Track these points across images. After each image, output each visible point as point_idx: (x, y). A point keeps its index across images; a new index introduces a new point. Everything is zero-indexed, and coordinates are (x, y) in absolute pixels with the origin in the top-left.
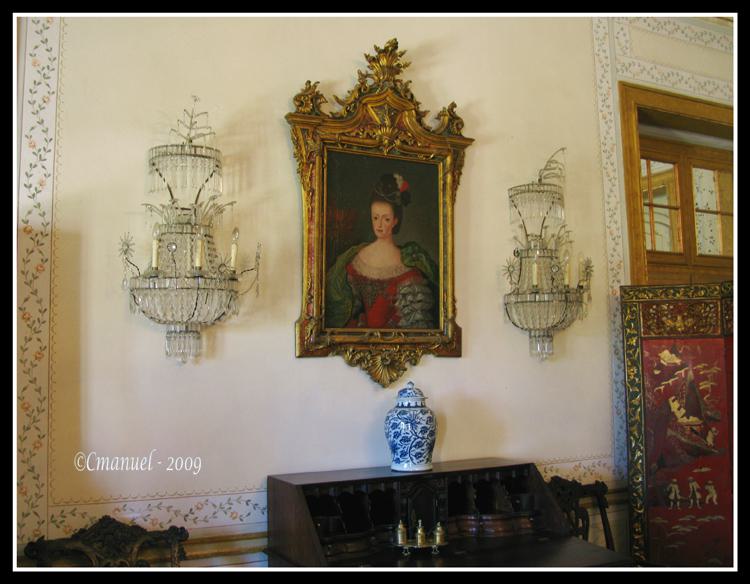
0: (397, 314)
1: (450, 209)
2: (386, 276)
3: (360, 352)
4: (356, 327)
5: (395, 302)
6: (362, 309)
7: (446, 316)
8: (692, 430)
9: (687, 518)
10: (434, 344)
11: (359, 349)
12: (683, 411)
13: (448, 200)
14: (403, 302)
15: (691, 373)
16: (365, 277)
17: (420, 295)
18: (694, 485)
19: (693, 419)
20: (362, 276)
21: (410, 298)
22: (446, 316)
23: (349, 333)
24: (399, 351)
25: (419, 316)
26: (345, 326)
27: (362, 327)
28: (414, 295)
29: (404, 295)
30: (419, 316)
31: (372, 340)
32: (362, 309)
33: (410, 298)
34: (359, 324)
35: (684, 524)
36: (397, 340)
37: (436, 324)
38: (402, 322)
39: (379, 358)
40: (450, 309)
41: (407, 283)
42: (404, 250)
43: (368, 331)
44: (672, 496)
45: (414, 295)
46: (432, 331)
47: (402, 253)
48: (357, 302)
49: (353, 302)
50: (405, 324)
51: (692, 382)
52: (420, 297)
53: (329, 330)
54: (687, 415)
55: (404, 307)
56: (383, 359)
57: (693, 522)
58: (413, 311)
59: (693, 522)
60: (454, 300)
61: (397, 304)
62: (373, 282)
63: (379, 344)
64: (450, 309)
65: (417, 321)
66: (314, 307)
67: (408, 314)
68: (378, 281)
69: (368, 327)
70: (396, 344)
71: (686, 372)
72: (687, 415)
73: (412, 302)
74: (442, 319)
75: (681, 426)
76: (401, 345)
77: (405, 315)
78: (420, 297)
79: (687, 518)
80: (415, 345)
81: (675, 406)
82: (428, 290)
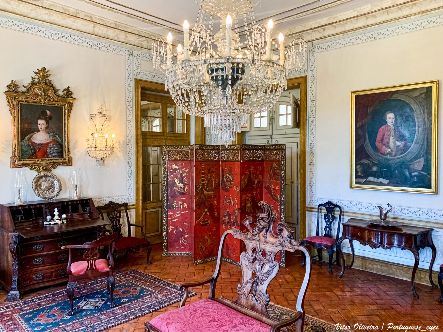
0: (48, 154)
1: (67, 121)
3: (34, 166)
4: (33, 158)
6: (35, 152)
7: (65, 154)
8: (181, 187)
9: (178, 212)
11: (34, 165)
12: (178, 182)
13: (66, 118)
14: (50, 150)
15: (181, 171)
18: (181, 203)
19: (181, 184)
21: (52, 149)
22: (65, 154)
23: (30, 160)
24: (49, 165)
25: (56, 154)
28: (54, 148)
29: (50, 148)
31: (38, 162)
32: (35, 152)
33: (52, 149)
35: (178, 214)
36: (47, 162)
38: (50, 156)
39: (41, 167)
40: (67, 152)
41: (52, 144)
43: (37, 159)
44: (174, 206)
45: (54, 148)
46: (61, 159)
48: (33, 151)
50: (51, 156)
51: (181, 174)
54: (179, 183)
56: (43, 168)
57: (180, 213)
58: (54, 152)
59: (180, 213)
60: (68, 149)
61: (48, 151)
62: (39, 144)
64: (67, 152)
65: (55, 156)
66: (16, 153)
69: (37, 158)
70: (47, 163)
71: (180, 171)
72: (179, 183)
73: (53, 150)
75: (178, 186)
77: (51, 154)
78: (56, 148)
79: (178, 212)
81: (176, 180)
82: (59, 146)
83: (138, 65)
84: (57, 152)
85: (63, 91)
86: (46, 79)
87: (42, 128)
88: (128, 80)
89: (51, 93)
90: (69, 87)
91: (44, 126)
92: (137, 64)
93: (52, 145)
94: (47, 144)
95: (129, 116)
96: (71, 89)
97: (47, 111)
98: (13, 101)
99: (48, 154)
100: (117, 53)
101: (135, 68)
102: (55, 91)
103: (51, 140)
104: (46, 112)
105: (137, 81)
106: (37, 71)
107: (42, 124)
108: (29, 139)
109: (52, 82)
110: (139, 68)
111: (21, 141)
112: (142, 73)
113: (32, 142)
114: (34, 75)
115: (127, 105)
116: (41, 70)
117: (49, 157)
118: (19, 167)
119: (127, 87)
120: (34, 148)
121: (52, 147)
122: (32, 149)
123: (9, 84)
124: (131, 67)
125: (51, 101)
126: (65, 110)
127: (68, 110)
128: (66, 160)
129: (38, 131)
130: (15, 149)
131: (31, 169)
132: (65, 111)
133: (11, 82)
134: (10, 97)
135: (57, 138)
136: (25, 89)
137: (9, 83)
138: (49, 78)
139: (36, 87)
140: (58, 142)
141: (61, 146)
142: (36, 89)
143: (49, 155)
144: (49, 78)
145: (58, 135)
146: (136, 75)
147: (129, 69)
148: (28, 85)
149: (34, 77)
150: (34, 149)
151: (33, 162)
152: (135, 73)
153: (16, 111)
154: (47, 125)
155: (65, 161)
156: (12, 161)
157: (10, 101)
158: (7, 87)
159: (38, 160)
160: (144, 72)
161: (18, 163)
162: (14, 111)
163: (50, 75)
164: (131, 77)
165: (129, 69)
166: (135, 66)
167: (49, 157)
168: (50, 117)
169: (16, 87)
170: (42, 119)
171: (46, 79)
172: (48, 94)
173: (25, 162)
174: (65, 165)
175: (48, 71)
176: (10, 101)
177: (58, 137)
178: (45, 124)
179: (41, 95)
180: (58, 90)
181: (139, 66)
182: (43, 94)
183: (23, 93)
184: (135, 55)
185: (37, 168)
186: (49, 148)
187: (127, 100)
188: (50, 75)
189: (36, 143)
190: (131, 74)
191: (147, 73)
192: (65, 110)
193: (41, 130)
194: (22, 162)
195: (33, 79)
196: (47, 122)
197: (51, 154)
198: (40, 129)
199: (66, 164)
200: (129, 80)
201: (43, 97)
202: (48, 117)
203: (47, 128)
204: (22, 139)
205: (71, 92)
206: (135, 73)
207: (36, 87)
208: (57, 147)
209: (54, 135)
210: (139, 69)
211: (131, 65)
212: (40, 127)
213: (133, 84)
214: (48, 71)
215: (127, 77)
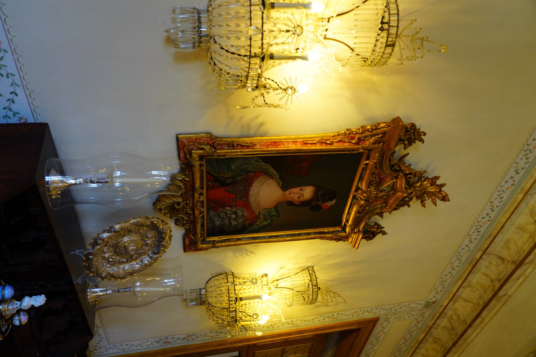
0: (220, 209)
2: (252, 199)
5: (231, 206)
7: (218, 242)
10: (194, 236)
16: (251, 186)
17: (235, 223)
20: (253, 182)
24: (187, 213)
25: (218, 223)
27: (207, 184)
28: (235, 219)
29: (235, 213)
30: (218, 223)
31: (196, 195)
33: (233, 216)
34: (210, 183)
37: (210, 234)
39: (180, 200)
41: (245, 214)
42: (273, 210)
43: (204, 191)
45: (235, 219)
46: (205, 235)
47: (271, 209)
48: (229, 181)
49: (229, 178)
50: (211, 215)
52: (234, 223)
53: (204, 163)
55: (226, 213)
56: (178, 204)
58: (223, 219)
61: (229, 208)
63: (193, 198)
65: (214, 222)
67: (220, 216)
69: (207, 190)
70: (193, 210)
73: (230, 218)
74: (216, 239)
76: (194, 214)
77: (218, 214)
78: (234, 223)
80: (193, 222)
87: (292, 195)
90: (384, 233)
92: (406, 316)
93: (243, 215)
94: (247, 205)
97: (334, 201)
100: (435, 287)
101: (398, 316)
103: (257, 213)
104: (332, 200)
106: (438, 182)
107: (303, 195)
109: (406, 207)
113: (256, 177)
117: (211, 211)
118: (182, 155)
121: (237, 216)
128: (202, 244)
129: (284, 188)
135: (261, 222)
136: (397, 156)
145: (269, 224)
151: (198, 184)
152: (389, 316)
154: (297, 203)
156: (200, 139)
158: (413, 125)
160: (388, 327)
161: (195, 156)
167: (211, 211)
168: (318, 208)
170: (315, 193)
174: (187, 242)
177: (265, 223)
178: (301, 199)
184: (424, 311)
186: (234, 210)
189: (250, 185)
190: (388, 311)
191: (386, 330)
193: (287, 192)
194: (197, 164)
197: (218, 214)
198: (290, 190)
202: (319, 203)
203: (290, 203)
209: (271, 216)
210: (396, 320)
212: (297, 190)
213: (368, 316)
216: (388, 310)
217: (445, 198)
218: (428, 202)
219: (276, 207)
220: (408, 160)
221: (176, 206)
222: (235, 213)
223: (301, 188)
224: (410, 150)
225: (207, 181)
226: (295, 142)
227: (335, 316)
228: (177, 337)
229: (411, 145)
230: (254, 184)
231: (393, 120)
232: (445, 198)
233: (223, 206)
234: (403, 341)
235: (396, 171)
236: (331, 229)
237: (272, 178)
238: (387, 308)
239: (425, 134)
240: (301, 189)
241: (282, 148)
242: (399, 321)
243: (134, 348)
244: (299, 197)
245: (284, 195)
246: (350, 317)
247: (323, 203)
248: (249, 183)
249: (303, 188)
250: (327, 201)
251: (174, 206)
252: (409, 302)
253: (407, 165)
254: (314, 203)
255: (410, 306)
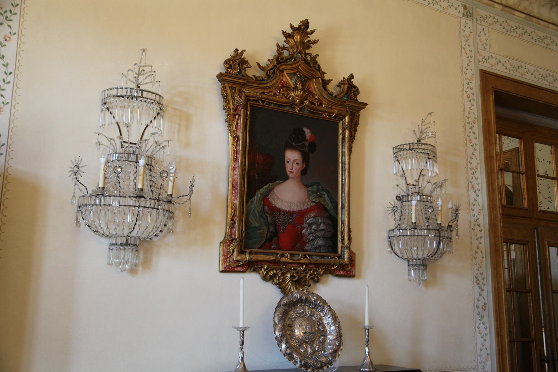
0: (304, 239)
1: (347, 158)
2: (295, 209)
3: (273, 269)
5: (302, 229)
6: (275, 234)
7: (343, 243)
10: (334, 266)
11: (272, 266)
13: (346, 151)
16: (279, 209)
17: (322, 225)
20: (275, 207)
21: (314, 227)
22: (343, 243)
23: (265, 254)
24: (305, 270)
25: (321, 242)
26: (261, 248)
27: (274, 249)
28: (318, 225)
29: (310, 225)
30: (321, 242)
31: (283, 259)
32: (275, 234)
33: (314, 227)
34: (273, 246)
36: (303, 261)
37: (335, 250)
38: (308, 246)
39: (289, 275)
40: (346, 238)
41: (313, 215)
42: (310, 189)
43: (280, 252)
45: (318, 225)
46: (332, 255)
47: (308, 191)
48: (272, 229)
49: (268, 229)
52: (322, 227)
53: (248, 251)
55: (309, 234)
56: (292, 277)
58: (317, 237)
60: (350, 231)
61: (304, 231)
62: (285, 213)
63: (289, 263)
64: (346, 238)
65: (320, 246)
66: (236, 231)
67: (313, 240)
68: (289, 212)
69: (279, 249)
70: (302, 264)
73: (316, 230)
74: (340, 245)
76: (306, 264)
77: (310, 241)
78: (322, 227)
80: (317, 265)
82: (328, 221)
83: (484, 41)
84: (324, 238)
85: (339, 85)
86: (307, 51)
87: (294, 170)
88: (467, 71)
89: (314, 86)
90: (352, 76)
91: (297, 167)
92: (483, 38)
93: (314, 217)
94: (302, 214)
95: (473, 157)
96: (355, 81)
97: (306, 130)
98: (237, 98)
99: (304, 239)
100: (442, 9)
101: (480, 47)
102: (325, 83)
103: (312, 204)
104: (304, 132)
105: (485, 76)
106: (290, 31)
107: (294, 161)
108: (265, 198)
109: (318, 59)
110: (487, 47)
111: (247, 202)
112: (494, 59)
113: (269, 204)
114: (282, 40)
115: (468, 130)
116: (299, 29)
117: (306, 248)
118: (239, 269)
119: (465, 89)
120: (274, 221)
121: (314, 223)
122: (268, 225)
123: (229, 57)
124: (471, 42)
125: (315, 104)
126: (344, 130)
127: (350, 132)
128: (344, 259)
129: (285, 178)
130: (232, 220)
131: (265, 278)
132: (343, 133)
133: (233, 54)
134: (231, 88)
135: (324, 200)
136: (259, 73)
137: (228, 54)
138: (313, 51)
139: (285, 69)
140: (326, 210)
141: (333, 221)
142: (285, 73)
143: (305, 243)
144: (313, 51)
145: (328, 193)
146: (481, 63)
147: (468, 48)
148: (269, 63)
149: (281, 45)
150: (275, 224)
151: (272, 258)
152: (480, 59)
153: (241, 122)
154: (305, 166)
155: (341, 261)
156: (224, 252)
157: (230, 97)
158: (226, 62)
159: (283, 255)
160: (498, 57)
161: (239, 258)
162: (237, 124)
163: (315, 42)
164: (472, 65)
165: (468, 48)
166: (479, 43)
167: (306, 248)
168: (312, 146)
169: (245, 66)
170: (293, 148)
171: (307, 51)
172: (308, 88)
173: (254, 257)
174: (342, 273)
175: (312, 32)
176: (230, 97)
177: (326, 196)
178: (300, 162)
179: (296, 88)
180: (329, 81)
181: (488, 43)
182: (299, 86)
183: (259, 80)
184: (478, 18)
185: (279, 277)
186: (307, 225)
187: (467, 120)
188: (315, 42)
189: (279, 210)
190: (472, 60)
191: (503, 60)
192: (344, 130)
193: (290, 175)
194: (247, 257)
195: (280, 49)
196: (305, 158)
197: (310, 241)
198: (288, 173)
199: (344, 270)
200: (470, 73)
201: (299, 93)
202: (307, 144)
203: (304, 172)
204: (250, 195)
205: (355, 87)
206: (480, 59)
207: (285, 69)
208: (324, 223)
209: (318, 190)
210: (488, 50)
211: (471, 38)
212: (288, 167)
213: (476, 83)
214: (312, 32)
215: (465, 65)
216: (469, 60)
217: (306, 24)
218: (312, 38)
219: (307, 186)
220: (264, 62)
221: (296, 279)
222: (310, 225)
223: (286, 163)
224: (252, 63)
225: (270, 249)
226: (234, 169)
227: (471, 120)
228: (477, 296)
229: (247, 61)
230: (278, 206)
231: (220, 81)
232: (306, 24)
233: (300, 236)
234: (526, 37)
235: (274, 73)
236: (341, 131)
237: (273, 189)
238: (466, 61)
239: (237, 50)
240: (288, 162)
241: (238, 181)
242: (490, 46)
243: (487, 344)
244: (297, 164)
245: (293, 178)
246: (475, 103)
247: (307, 141)
248: (275, 210)
249: (286, 160)
250: (305, 136)
251: (296, 281)
252: (460, 37)
253: (269, 63)
254: (306, 149)
255: (467, 35)
